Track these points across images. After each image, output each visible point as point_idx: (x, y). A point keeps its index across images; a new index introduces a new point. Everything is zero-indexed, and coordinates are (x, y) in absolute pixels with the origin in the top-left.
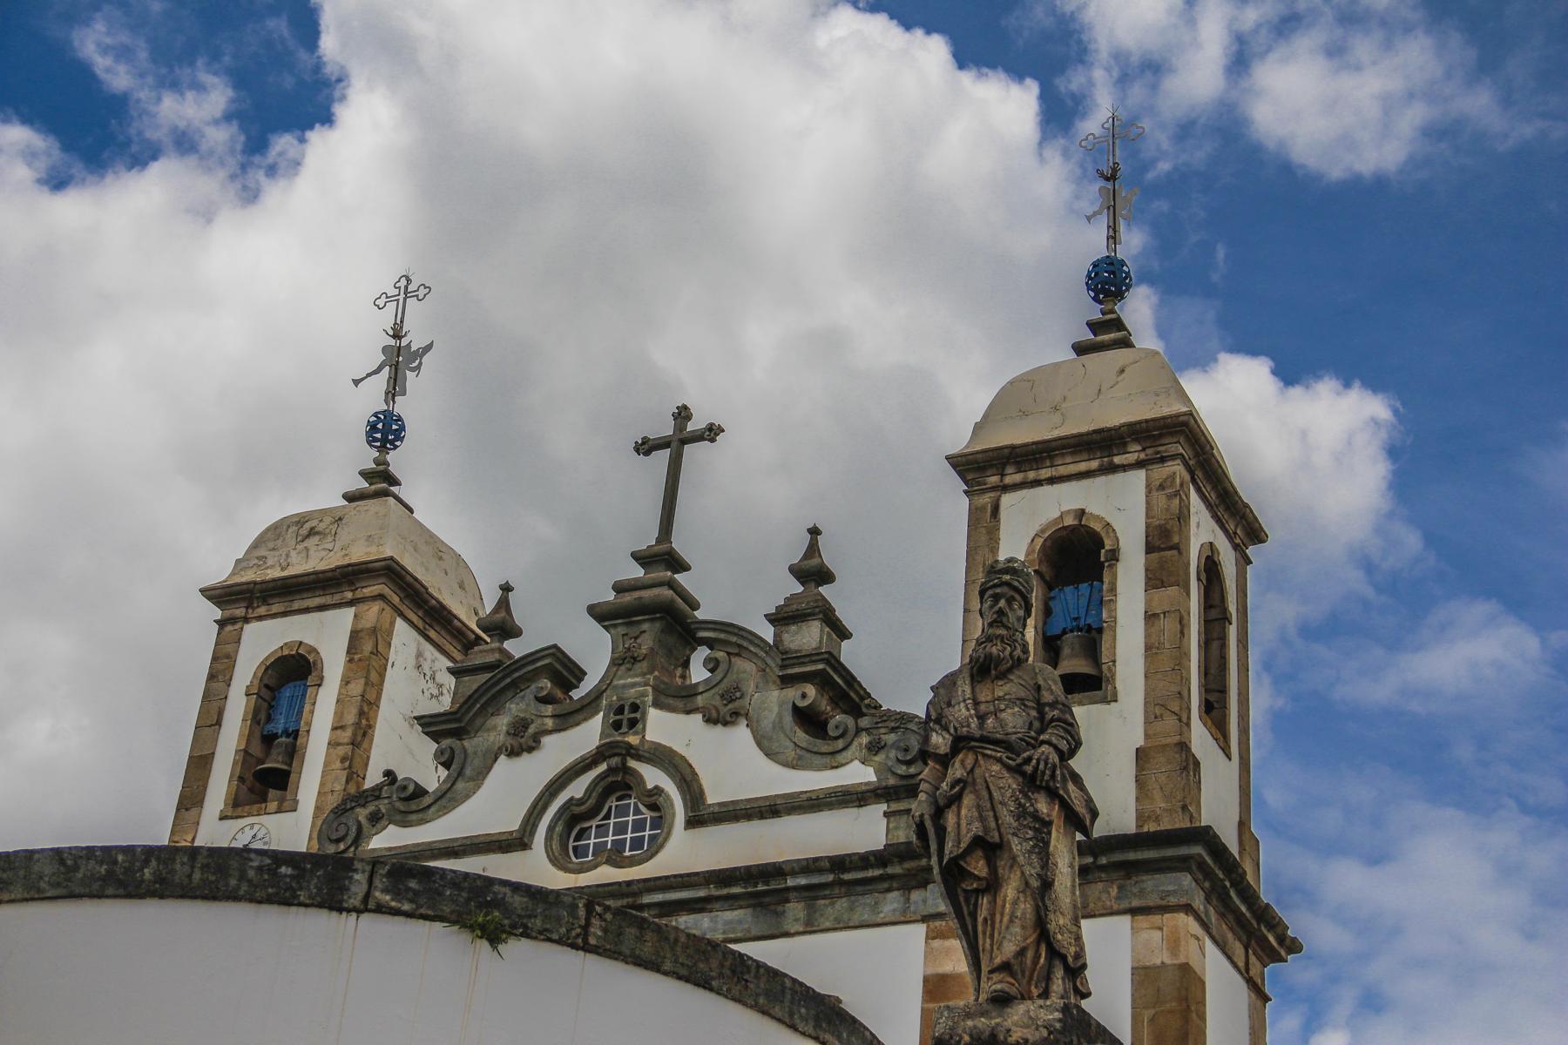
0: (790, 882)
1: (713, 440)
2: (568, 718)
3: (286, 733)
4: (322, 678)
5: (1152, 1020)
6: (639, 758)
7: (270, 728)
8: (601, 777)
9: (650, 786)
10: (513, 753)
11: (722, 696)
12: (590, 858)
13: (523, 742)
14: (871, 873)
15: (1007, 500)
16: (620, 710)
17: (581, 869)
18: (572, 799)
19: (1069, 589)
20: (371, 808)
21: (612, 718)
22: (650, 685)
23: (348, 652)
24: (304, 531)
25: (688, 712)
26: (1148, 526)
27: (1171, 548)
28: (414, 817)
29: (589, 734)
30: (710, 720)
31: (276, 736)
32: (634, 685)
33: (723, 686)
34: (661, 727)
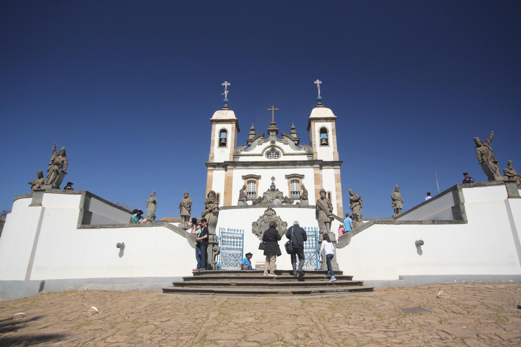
2: (265, 142)
7: (220, 138)
8: (271, 149)
9: (277, 150)
13: (260, 144)
15: (316, 123)
16: (272, 141)
17: (270, 159)
18: (268, 151)
19: (323, 134)
20: (240, 149)
23: (232, 129)
26: (332, 129)
29: (268, 144)
30: (284, 144)
31: (222, 139)
33: (285, 140)
34: (277, 144)
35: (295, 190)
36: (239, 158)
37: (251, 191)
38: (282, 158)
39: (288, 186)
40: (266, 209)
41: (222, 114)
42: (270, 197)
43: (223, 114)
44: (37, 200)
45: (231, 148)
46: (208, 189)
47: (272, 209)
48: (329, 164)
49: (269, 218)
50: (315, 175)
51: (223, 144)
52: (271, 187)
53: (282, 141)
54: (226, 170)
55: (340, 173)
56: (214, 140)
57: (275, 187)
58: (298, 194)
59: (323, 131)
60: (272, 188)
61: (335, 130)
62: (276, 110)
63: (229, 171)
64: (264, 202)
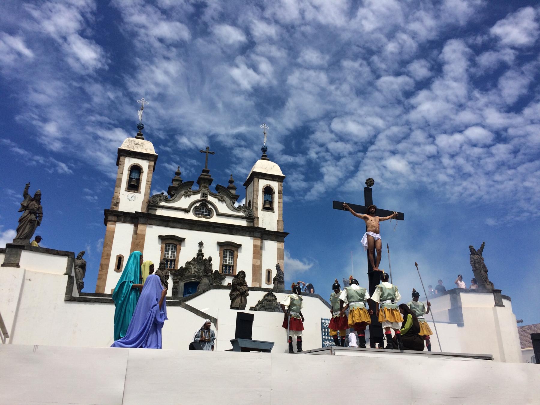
0: (235, 228)
1: (213, 154)
2: (195, 193)
3: (134, 178)
4: (143, 171)
5: (280, 255)
6: (207, 203)
7: (131, 176)
10: (186, 196)
11: (221, 197)
12: (198, 215)
13: (187, 195)
14: (247, 229)
15: (260, 180)
16: (204, 194)
17: (199, 217)
18: (196, 206)
19: (267, 195)
20: (159, 198)
21: (203, 195)
22: (208, 191)
23: (148, 168)
24: (136, 143)
25: (215, 198)
27: (281, 194)
28: (168, 202)
29: (198, 197)
30: (219, 200)
31: (132, 178)
32: (205, 191)
33: (221, 196)
34: (210, 198)
35: (228, 263)
36: (157, 209)
37: (169, 258)
38: (215, 219)
39: (219, 258)
40: (266, 293)
41: (136, 145)
42: (196, 270)
43: (137, 144)
44: (12, 259)
45: (145, 195)
46: (106, 248)
47: (273, 293)
48: (271, 234)
49: (269, 305)
50: (255, 246)
51: (133, 186)
52: (198, 255)
53: (217, 197)
54: (136, 226)
55: (283, 248)
56: (122, 179)
57: (203, 256)
58: (231, 269)
59: (268, 191)
60: (200, 256)
61: (282, 193)
62: (211, 153)
63: (140, 227)
64: (186, 275)
